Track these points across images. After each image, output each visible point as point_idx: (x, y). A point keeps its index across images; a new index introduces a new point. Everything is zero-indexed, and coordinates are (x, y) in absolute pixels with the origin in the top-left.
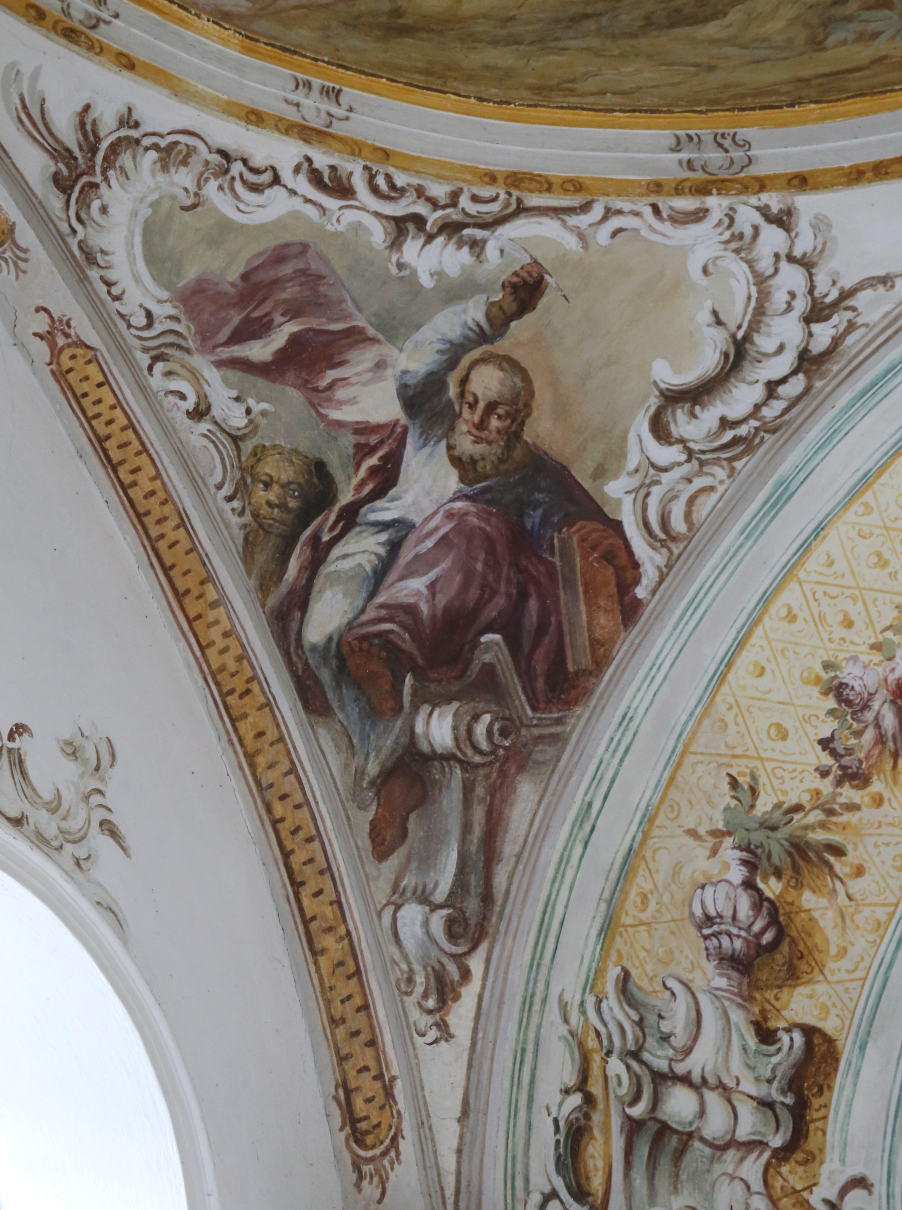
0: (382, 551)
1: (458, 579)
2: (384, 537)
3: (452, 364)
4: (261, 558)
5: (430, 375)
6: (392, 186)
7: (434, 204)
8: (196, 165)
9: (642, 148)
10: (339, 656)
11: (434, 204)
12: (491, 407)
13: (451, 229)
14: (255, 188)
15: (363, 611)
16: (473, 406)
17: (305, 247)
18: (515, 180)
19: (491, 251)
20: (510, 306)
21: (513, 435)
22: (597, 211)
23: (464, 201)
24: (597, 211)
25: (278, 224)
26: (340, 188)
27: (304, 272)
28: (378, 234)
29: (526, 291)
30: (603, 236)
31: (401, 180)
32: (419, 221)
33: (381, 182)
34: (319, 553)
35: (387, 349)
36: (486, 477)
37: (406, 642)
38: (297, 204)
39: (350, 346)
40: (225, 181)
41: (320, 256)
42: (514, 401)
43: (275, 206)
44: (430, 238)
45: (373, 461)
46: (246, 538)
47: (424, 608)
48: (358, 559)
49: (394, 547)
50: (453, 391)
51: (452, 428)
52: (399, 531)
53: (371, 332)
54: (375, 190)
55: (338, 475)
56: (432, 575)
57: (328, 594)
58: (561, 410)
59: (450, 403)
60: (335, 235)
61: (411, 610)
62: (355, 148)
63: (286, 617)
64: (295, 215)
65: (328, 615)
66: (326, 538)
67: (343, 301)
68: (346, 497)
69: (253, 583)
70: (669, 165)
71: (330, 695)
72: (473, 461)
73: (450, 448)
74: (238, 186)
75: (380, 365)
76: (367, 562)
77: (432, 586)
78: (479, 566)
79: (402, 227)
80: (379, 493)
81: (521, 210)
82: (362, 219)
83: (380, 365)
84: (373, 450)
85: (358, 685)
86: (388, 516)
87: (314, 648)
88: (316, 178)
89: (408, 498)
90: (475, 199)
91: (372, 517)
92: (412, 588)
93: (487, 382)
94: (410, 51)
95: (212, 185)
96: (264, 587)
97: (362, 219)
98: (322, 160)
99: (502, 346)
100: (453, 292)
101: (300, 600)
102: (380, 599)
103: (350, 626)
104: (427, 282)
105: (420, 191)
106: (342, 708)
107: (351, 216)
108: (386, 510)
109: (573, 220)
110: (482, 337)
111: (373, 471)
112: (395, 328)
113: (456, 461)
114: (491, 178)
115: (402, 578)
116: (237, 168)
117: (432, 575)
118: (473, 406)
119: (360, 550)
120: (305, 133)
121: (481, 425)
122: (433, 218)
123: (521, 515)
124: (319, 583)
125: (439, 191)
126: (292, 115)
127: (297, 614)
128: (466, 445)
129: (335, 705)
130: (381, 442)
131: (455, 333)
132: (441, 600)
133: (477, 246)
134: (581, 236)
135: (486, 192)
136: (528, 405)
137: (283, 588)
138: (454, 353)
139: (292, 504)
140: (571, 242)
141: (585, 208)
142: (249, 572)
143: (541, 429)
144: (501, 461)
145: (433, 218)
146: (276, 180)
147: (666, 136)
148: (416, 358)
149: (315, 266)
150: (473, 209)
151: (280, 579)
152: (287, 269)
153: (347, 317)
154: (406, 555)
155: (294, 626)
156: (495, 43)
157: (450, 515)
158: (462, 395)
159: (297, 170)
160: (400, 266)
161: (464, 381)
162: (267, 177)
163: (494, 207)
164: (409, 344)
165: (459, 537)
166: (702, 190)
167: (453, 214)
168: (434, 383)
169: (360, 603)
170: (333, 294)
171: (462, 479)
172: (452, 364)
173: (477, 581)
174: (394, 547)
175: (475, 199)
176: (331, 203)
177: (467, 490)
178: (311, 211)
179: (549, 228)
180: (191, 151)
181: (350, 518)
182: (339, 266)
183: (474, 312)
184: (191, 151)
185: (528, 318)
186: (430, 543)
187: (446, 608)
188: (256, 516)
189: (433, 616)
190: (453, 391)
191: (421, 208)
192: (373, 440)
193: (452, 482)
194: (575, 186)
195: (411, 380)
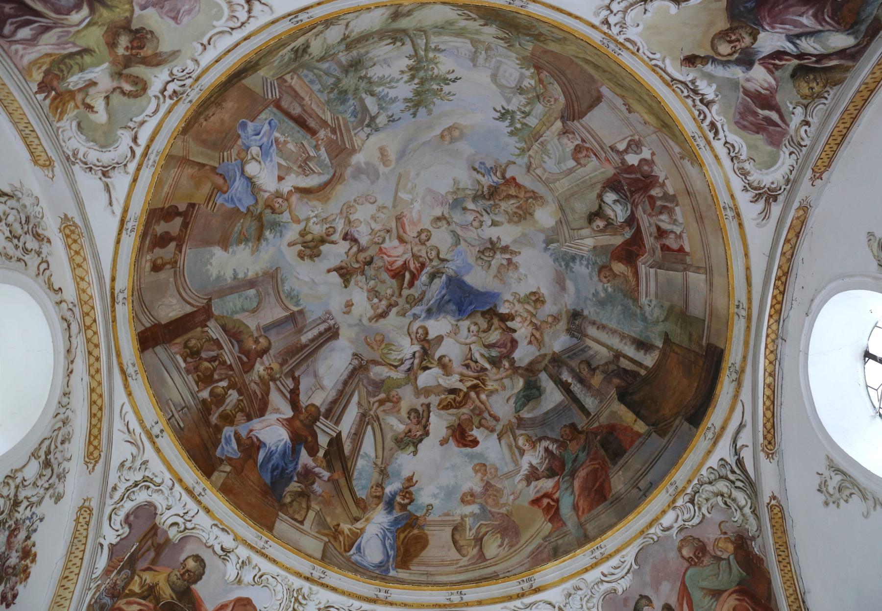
0: (803, 39)
1: (791, 10)
2: (798, 42)
3: (729, 62)
4: (838, 76)
5: (738, 65)
6: (700, 114)
7: (694, 100)
8: (741, 165)
9: (626, 59)
10: (852, 27)
11: (694, 100)
12: (730, 42)
13: (696, 92)
14: (733, 146)
15: (829, 30)
16: (735, 47)
17: (736, 123)
18: (668, 85)
19: (690, 77)
20: (698, 61)
21: (732, 30)
22: (654, 62)
23: (686, 94)
24: (654, 62)
25: (736, 134)
26: (713, 125)
27: (743, 118)
28: (715, 108)
29: (691, 60)
30: (658, 56)
31: (697, 113)
32: (702, 101)
33: (702, 117)
34: (821, 58)
35: (742, 81)
36: (751, 27)
37: (828, 9)
38: (727, 133)
39: (751, 92)
40: (738, 155)
41: (734, 117)
42: (722, 37)
43: (732, 138)
44: (703, 95)
45: (777, 62)
46: (835, 85)
47: (811, 12)
48: (813, 44)
49: (798, 36)
50: (736, 56)
51: (747, 47)
52: (791, 38)
53: (741, 90)
54: (705, 117)
55: (791, 69)
56: (797, 18)
57: (832, 45)
58: (711, 24)
59: (740, 54)
60: (725, 117)
61: (815, 16)
62: (700, 128)
63: (852, 55)
64: (730, 131)
65: (841, 41)
66: (814, 59)
67: (741, 103)
68: (796, 62)
69: (848, 75)
70: (625, 53)
71: (869, 21)
72: (750, 34)
73: (753, 44)
74: (737, 151)
75: (748, 80)
76: (811, 41)
77: (801, 15)
78: (781, 7)
79: (708, 104)
80: (785, 53)
81: (673, 79)
82: (714, 113)
83: (748, 80)
84: (774, 64)
85: (858, 14)
86: (790, 45)
87: (856, 38)
88: (716, 133)
89: (779, 43)
90: (682, 92)
91: (795, 49)
92: (807, 21)
93: (724, 48)
94: (667, 119)
95: (742, 158)
96: (848, 69)
97: (714, 113)
98: (711, 135)
99: (711, 53)
100: (710, 78)
101: (842, 53)
102: (820, 28)
103: (837, 31)
104: (714, 86)
105: (694, 106)
106: (871, 14)
107: (717, 118)
108: (789, 47)
109: (662, 66)
110: (714, 60)
111: (780, 60)
112: (735, 84)
113: (755, 39)
114: (673, 90)
115: (807, 26)
116: (732, 154)
117: (797, 18)
118: (735, 47)
119: (808, 45)
120: (709, 143)
121: (738, 40)
122: (697, 98)
123: (752, 9)
124: (832, 51)
125: (689, 101)
126: (707, 147)
127: (848, 51)
128: (748, 40)
129: (872, 17)
130: (770, 64)
131: (720, 68)
132: (803, 9)
133: (693, 82)
134: (664, 61)
135: (678, 90)
136: (720, 33)
137: (842, 62)
138: (725, 64)
139: (812, 77)
140: (668, 61)
141: (656, 65)
142: (846, 78)
143: (722, 24)
144: (742, 27)
145: (697, 98)
146: (726, 142)
147: (620, 57)
148: (737, 73)
149: (738, 117)
150: (685, 91)
151: (840, 65)
152: (746, 123)
153: (743, 98)
154: (798, 30)
155: (853, 50)
156: (646, 101)
157: (773, 28)
158: (734, 52)
159: (719, 139)
160: (717, 96)
161: (730, 55)
162: (728, 145)
163: (679, 86)
164: (735, 77)
165: (777, 19)
166: (621, 43)
167: (691, 94)
168: (738, 62)
169: (827, 33)
170: (741, 107)
171: (759, 33)
172: (729, 62)
173: (786, 4)
174: (798, 36)
175: (682, 92)
176: (719, 125)
177: (760, 29)
178: (726, 128)
179: (670, 69)
180: (739, 169)
181: (801, 56)
182: (732, 110)
183: (709, 68)
184: (739, 169)
185: (697, 53)
186: (787, 27)
187: (805, 6)
188: (825, 86)
189: (811, 8)
190: (736, 56)
191: (698, 103)
192: (771, 66)
193: (762, 35)
194: (654, 70)
195: (744, 69)
